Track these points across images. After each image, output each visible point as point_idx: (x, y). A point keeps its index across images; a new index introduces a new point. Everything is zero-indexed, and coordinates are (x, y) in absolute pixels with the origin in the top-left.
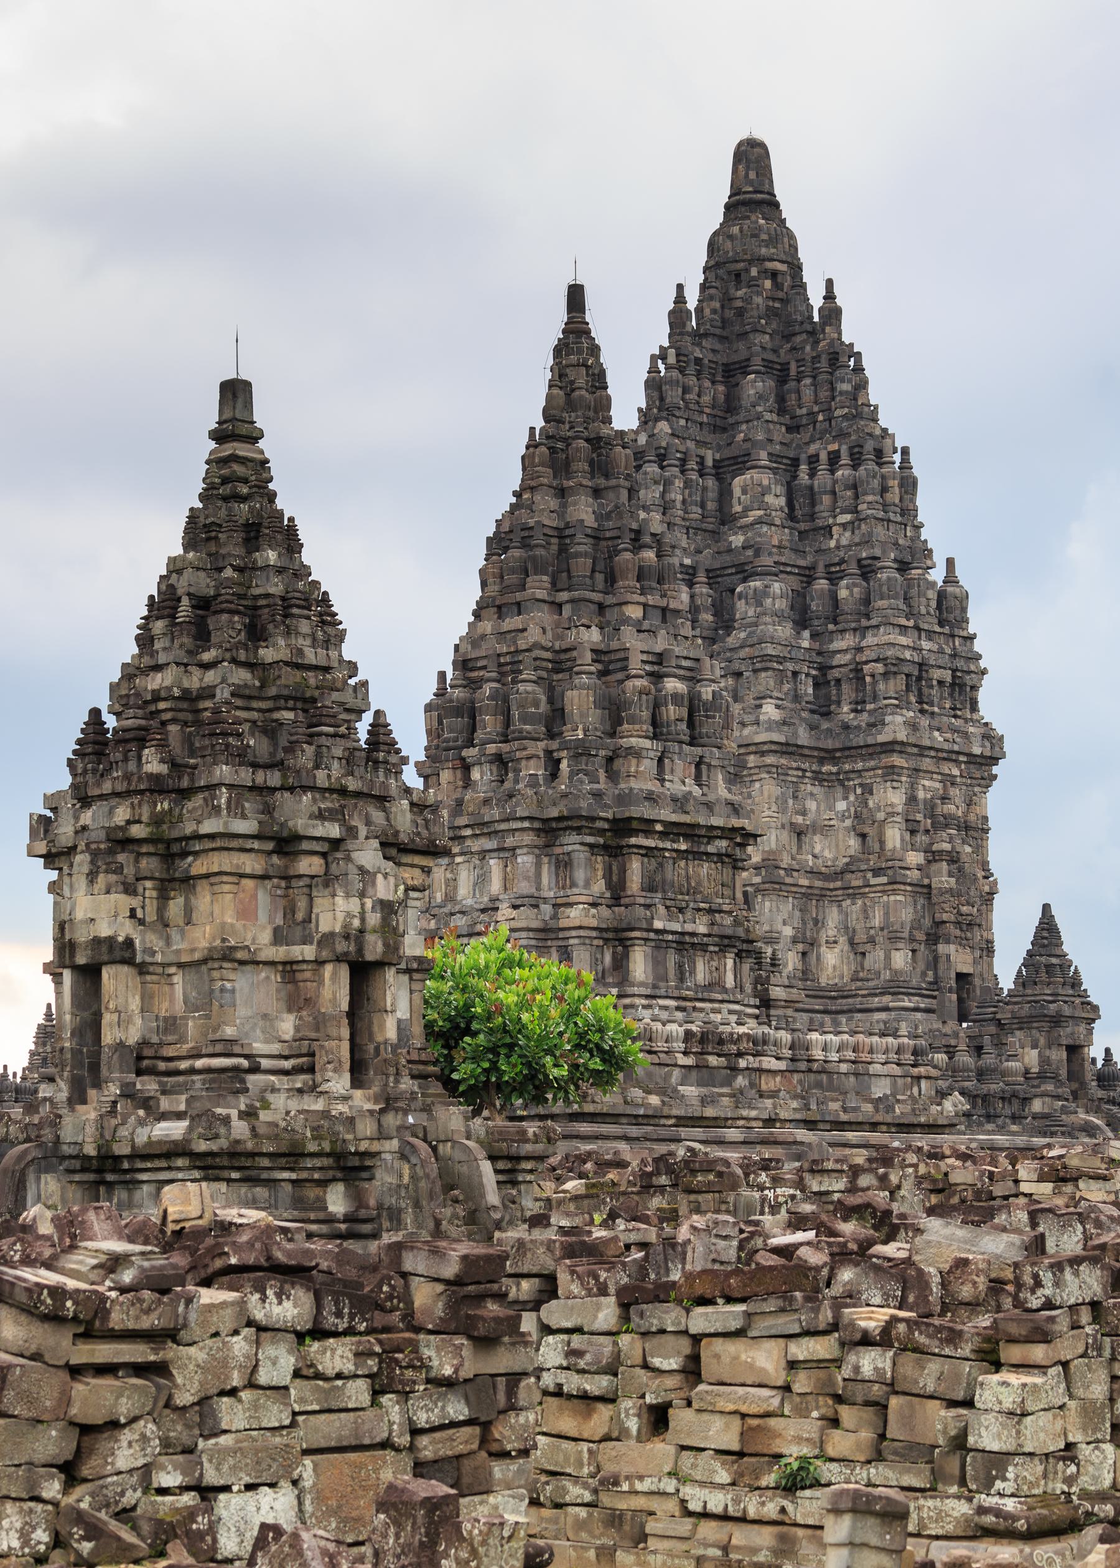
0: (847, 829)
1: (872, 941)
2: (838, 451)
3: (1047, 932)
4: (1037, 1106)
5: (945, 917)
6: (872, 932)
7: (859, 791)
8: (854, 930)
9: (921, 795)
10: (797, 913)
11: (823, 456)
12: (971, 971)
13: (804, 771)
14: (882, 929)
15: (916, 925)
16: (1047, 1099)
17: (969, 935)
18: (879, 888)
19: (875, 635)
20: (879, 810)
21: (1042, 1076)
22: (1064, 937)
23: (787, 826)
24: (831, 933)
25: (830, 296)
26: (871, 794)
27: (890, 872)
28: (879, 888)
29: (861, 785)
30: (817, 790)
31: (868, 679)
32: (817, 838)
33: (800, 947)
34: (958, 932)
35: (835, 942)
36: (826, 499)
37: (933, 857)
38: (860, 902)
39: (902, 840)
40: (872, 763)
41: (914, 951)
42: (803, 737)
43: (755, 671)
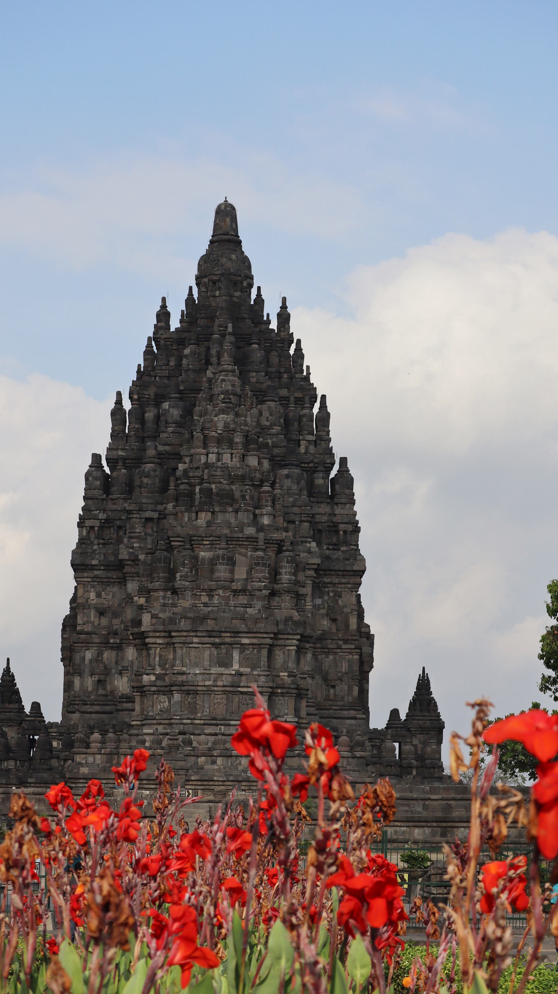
0: (323, 616)
2: (303, 398)
6: (340, 674)
7: (331, 594)
8: (327, 673)
11: (292, 399)
14: (346, 673)
18: (348, 650)
19: (343, 509)
20: (346, 606)
25: (284, 307)
26: (340, 596)
28: (346, 650)
29: (333, 591)
31: (341, 533)
36: (296, 424)
38: (331, 657)
40: (344, 581)
43: (301, 521)
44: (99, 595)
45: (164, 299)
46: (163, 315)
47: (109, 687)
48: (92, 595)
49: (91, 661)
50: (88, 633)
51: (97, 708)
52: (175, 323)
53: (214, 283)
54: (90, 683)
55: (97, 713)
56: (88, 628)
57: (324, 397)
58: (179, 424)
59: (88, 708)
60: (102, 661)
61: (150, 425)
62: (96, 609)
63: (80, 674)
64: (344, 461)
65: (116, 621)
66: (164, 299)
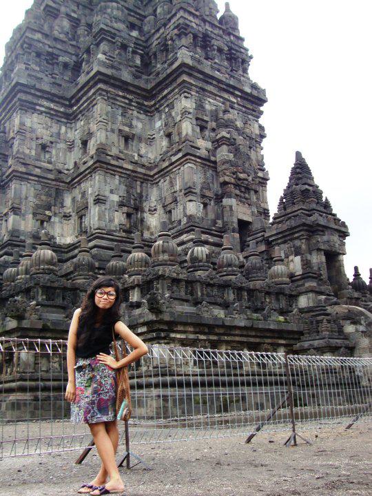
0: (161, 137)
1: (175, 201)
3: (301, 171)
4: (303, 302)
5: (227, 179)
9: (208, 107)
10: (123, 187)
12: (250, 220)
13: (131, 100)
15: (206, 186)
16: (311, 295)
17: (247, 195)
21: (305, 277)
22: (314, 174)
23: (117, 132)
24: (153, 205)
27: (189, 154)
30: (142, 116)
32: (143, 145)
33: (125, 209)
34: (238, 192)
35: (155, 210)
37: (218, 143)
39: (193, 130)
41: (205, 205)
42: (126, 76)
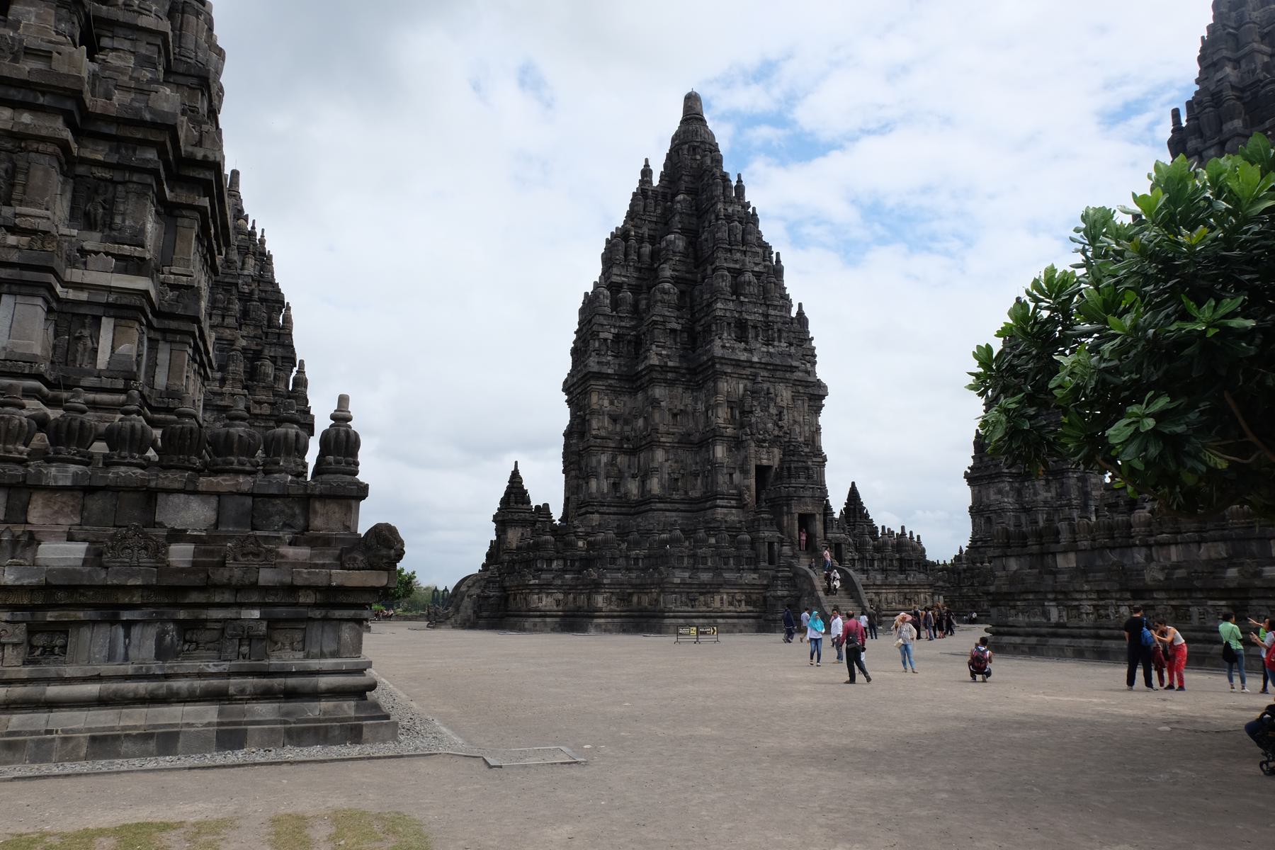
3: (854, 495)
25: (740, 181)
44: (612, 403)
45: (647, 160)
46: (646, 172)
47: (623, 490)
48: (606, 403)
49: (606, 465)
50: (603, 438)
51: (613, 510)
52: (656, 181)
53: (694, 148)
54: (605, 485)
55: (614, 514)
56: (603, 433)
57: (778, 254)
58: (685, 255)
59: (604, 509)
60: (615, 465)
61: (647, 259)
62: (610, 416)
63: (597, 477)
64: (800, 305)
65: (627, 428)
66: (647, 160)
